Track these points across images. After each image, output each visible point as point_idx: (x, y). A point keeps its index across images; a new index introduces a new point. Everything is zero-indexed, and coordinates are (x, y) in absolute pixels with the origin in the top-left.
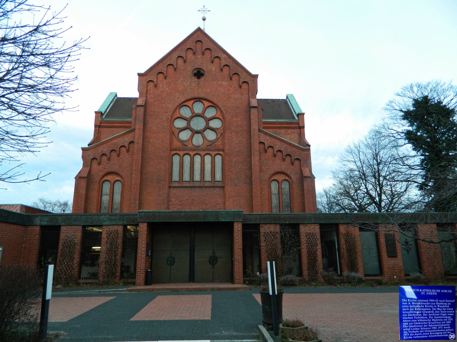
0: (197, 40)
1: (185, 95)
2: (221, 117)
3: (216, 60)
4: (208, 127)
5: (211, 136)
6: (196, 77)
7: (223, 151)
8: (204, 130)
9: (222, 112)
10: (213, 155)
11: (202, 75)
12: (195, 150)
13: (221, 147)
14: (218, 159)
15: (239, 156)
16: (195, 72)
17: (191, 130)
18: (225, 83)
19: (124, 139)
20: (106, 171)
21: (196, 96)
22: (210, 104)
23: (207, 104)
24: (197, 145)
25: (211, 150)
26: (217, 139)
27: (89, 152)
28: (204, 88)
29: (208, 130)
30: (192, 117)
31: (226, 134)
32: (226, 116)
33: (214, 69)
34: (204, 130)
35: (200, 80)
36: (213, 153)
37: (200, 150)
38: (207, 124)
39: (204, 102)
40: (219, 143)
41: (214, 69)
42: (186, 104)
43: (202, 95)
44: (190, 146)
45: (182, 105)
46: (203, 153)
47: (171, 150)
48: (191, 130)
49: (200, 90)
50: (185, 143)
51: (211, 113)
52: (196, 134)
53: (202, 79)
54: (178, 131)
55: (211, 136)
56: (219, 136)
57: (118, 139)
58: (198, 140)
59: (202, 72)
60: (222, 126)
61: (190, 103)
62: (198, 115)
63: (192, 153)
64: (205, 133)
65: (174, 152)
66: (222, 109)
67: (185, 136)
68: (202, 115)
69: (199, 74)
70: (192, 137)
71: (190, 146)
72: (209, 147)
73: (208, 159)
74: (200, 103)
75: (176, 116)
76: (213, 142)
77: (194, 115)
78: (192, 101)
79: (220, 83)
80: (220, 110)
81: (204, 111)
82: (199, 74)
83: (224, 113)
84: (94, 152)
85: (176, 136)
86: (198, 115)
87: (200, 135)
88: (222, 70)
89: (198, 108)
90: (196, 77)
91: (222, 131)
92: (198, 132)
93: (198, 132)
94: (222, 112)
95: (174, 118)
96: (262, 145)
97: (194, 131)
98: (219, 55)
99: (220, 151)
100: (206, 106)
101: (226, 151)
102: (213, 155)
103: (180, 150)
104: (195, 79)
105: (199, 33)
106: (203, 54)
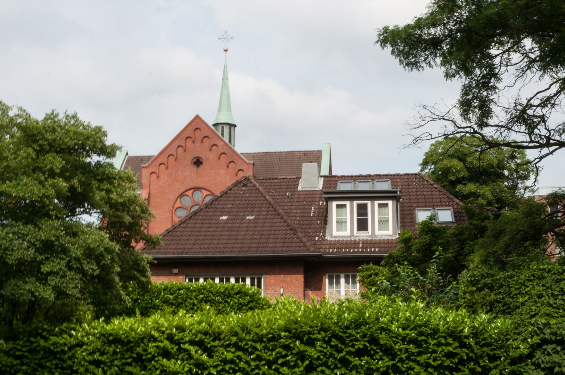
0: (196, 127)
3: (214, 147)
11: (201, 163)
16: (195, 160)
18: (222, 172)
21: (195, 185)
22: (208, 193)
33: (212, 157)
41: (212, 157)
42: (186, 193)
43: (200, 185)
49: (199, 179)
53: (202, 167)
69: (198, 162)
77: (194, 204)
78: (192, 191)
82: (198, 162)
88: (219, 158)
98: (217, 143)
100: (204, 195)
104: (194, 168)
105: (197, 119)
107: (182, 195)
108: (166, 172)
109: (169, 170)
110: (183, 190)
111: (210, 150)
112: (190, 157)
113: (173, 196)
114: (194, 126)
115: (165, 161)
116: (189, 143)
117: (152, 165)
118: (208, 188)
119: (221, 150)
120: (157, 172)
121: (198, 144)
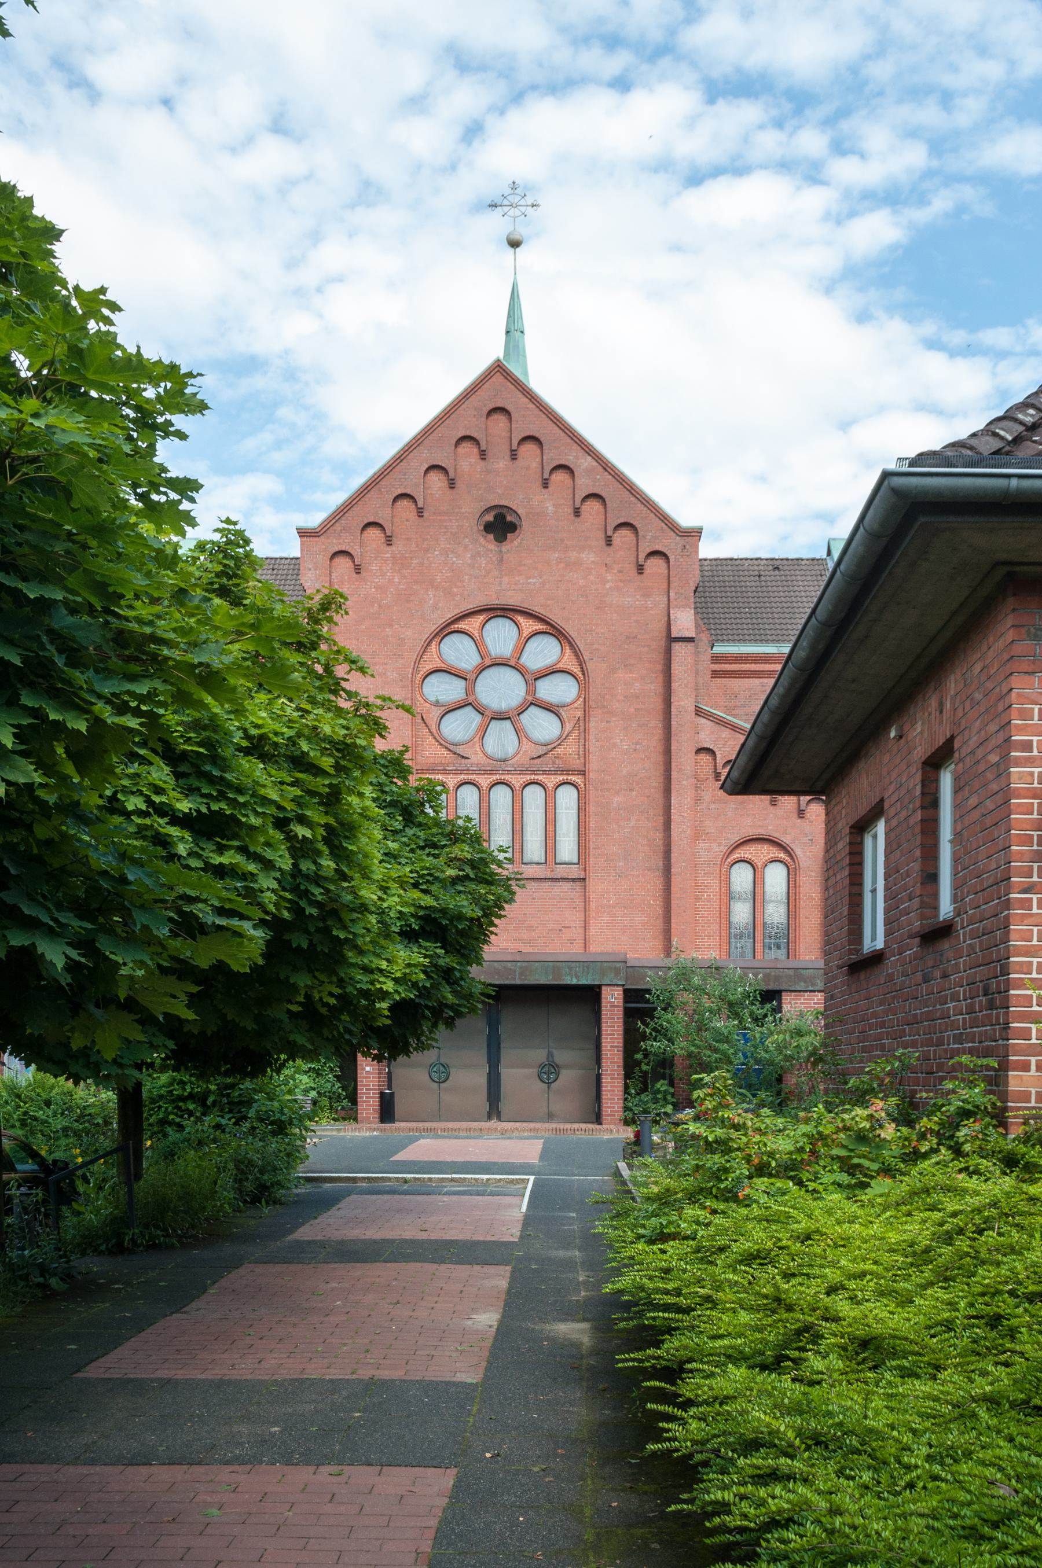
2: (576, 670)
3: (559, 477)
4: (533, 702)
5: (543, 727)
6: (491, 536)
7: (583, 773)
8: (522, 710)
9: (577, 653)
10: (550, 785)
11: (512, 528)
12: (492, 772)
13: (577, 764)
14: (567, 798)
15: (632, 790)
17: (480, 710)
21: (494, 601)
22: (540, 627)
23: (529, 626)
24: (500, 755)
25: (545, 773)
26: (561, 739)
28: (522, 571)
29: (532, 708)
30: (482, 669)
31: (592, 724)
32: (590, 666)
34: (522, 710)
35: (505, 547)
36: (551, 781)
37: (509, 772)
38: (531, 690)
39: (520, 619)
40: (570, 750)
42: (462, 625)
43: (512, 599)
44: (477, 758)
46: (517, 781)
48: (480, 710)
49: (505, 580)
50: (460, 750)
51: (543, 652)
52: (494, 723)
54: (436, 712)
55: (543, 727)
56: (568, 727)
58: (501, 741)
60: (579, 696)
61: (472, 624)
62: (500, 663)
63: (484, 781)
64: (525, 718)
66: (581, 644)
67: (459, 727)
68: (512, 663)
70: (483, 731)
71: (477, 758)
72: (535, 761)
73: (534, 797)
74: (508, 622)
75: (429, 667)
76: (551, 747)
77: (488, 662)
79: (573, 555)
80: (571, 646)
81: (520, 649)
82: (501, 525)
83: (586, 655)
85: (433, 727)
86: (500, 663)
87: (507, 724)
88: (577, 512)
89: (501, 637)
91: (579, 714)
92: (500, 717)
93: (500, 717)
94: (577, 653)
95: (423, 671)
96: (705, 758)
98: (569, 460)
99: (575, 774)
100: (526, 633)
101: (592, 776)
102: (550, 785)
103: (445, 772)
106: (514, 455)
107: (445, 631)
108: (388, 553)
109: (398, 547)
110: (449, 615)
111: (545, 484)
112: (470, 508)
113: (415, 634)
114: (486, 400)
115: (382, 516)
116: (467, 459)
117: (338, 527)
118: (538, 609)
119: (585, 485)
120: (356, 551)
121: (501, 463)
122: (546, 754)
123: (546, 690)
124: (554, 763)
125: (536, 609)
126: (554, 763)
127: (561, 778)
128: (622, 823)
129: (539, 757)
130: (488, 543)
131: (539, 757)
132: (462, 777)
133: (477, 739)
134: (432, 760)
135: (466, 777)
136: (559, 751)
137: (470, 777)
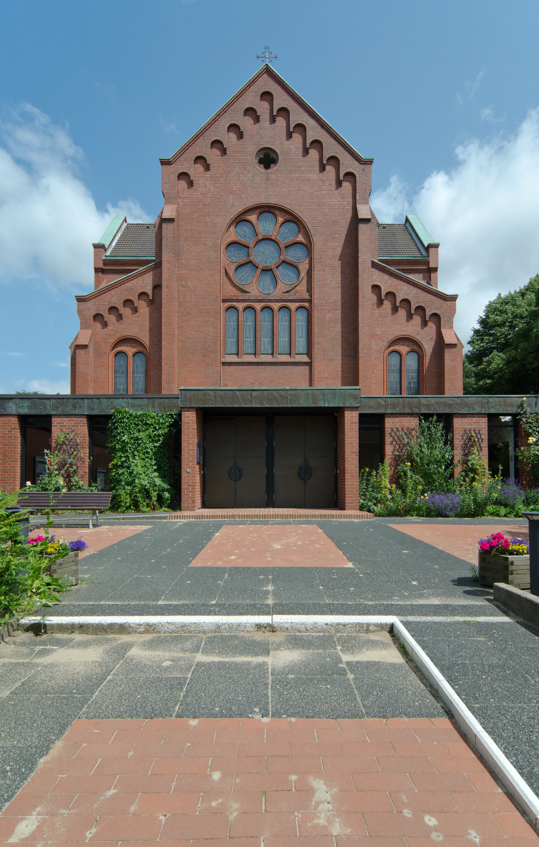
1: (245, 200)
6: (262, 166)
13: (306, 296)
19: (143, 281)
20: (118, 336)
22: (288, 217)
27: (89, 304)
36: (293, 306)
37: (271, 301)
39: (277, 212)
43: (273, 201)
45: (238, 220)
47: (224, 301)
54: (234, 266)
57: (135, 281)
59: (273, 155)
61: (253, 218)
65: (229, 304)
68: (273, 238)
72: (286, 294)
77: (260, 237)
82: (268, 159)
84: (97, 303)
90: (262, 166)
97: (260, 266)
122: (291, 290)
123: (292, 255)
124: (295, 295)
125: (286, 206)
126: (295, 295)
127: (299, 304)
128: (331, 329)
129: (287, 292)
130: (261, 168)
131: (287, 292)
132: (247, 303)
133: (254, 282)
134: (231, 294)
135: (248, 303)
136: (297, 288)
137: (250, 303)
